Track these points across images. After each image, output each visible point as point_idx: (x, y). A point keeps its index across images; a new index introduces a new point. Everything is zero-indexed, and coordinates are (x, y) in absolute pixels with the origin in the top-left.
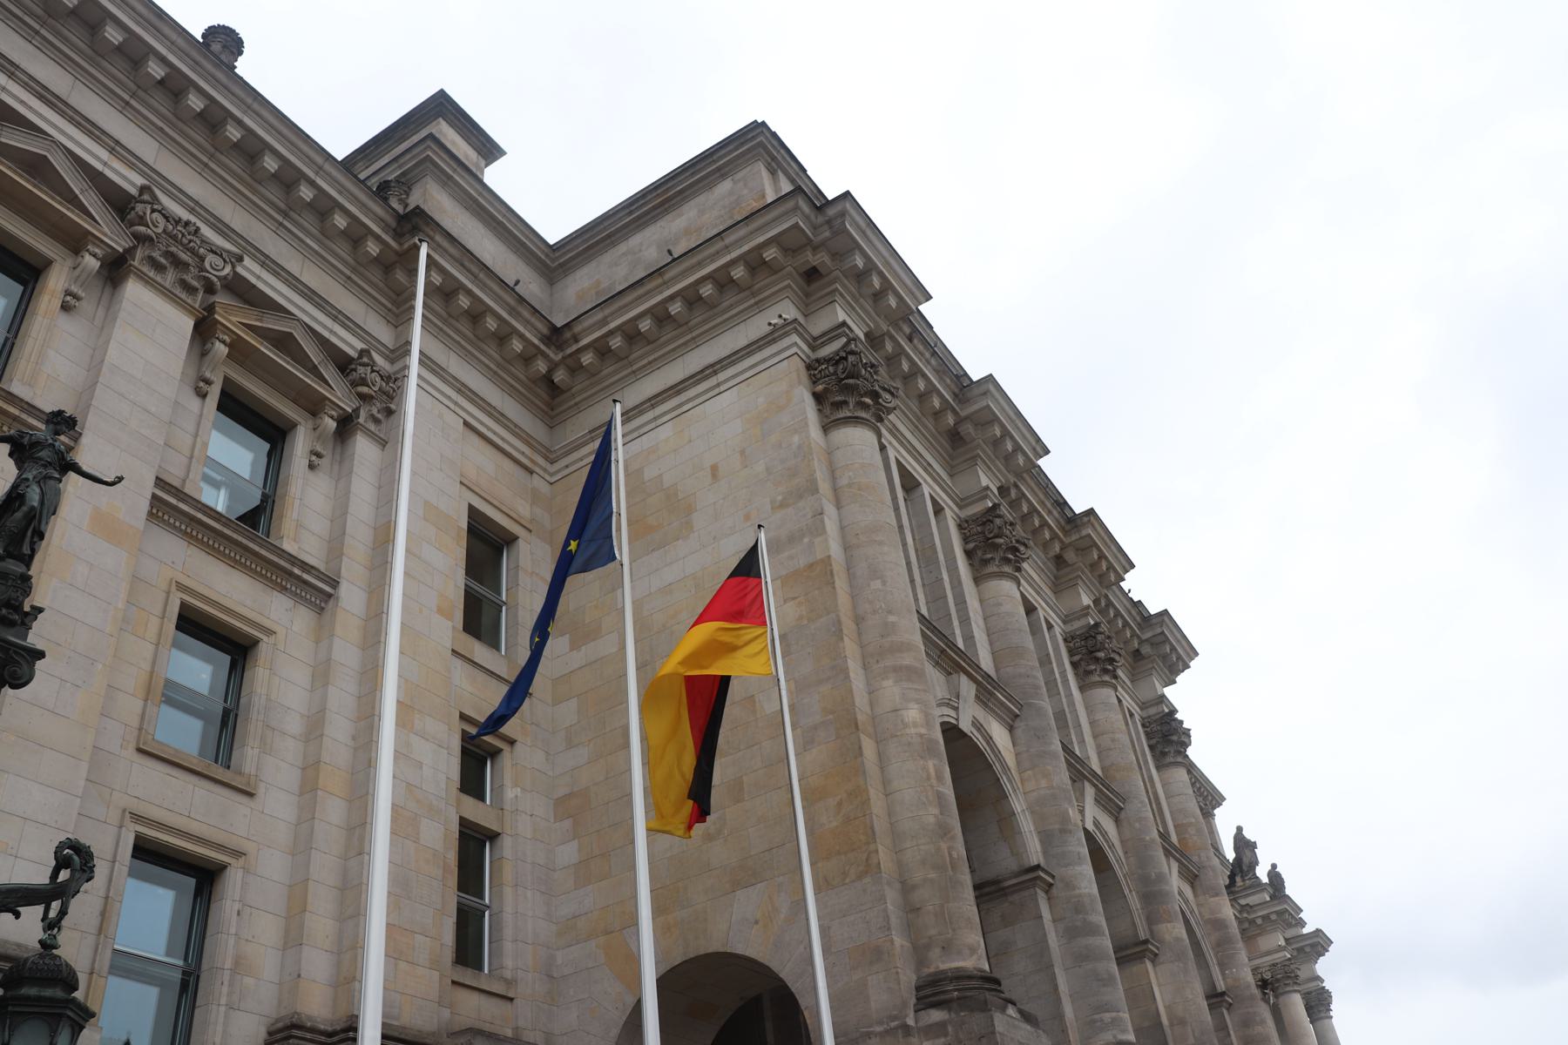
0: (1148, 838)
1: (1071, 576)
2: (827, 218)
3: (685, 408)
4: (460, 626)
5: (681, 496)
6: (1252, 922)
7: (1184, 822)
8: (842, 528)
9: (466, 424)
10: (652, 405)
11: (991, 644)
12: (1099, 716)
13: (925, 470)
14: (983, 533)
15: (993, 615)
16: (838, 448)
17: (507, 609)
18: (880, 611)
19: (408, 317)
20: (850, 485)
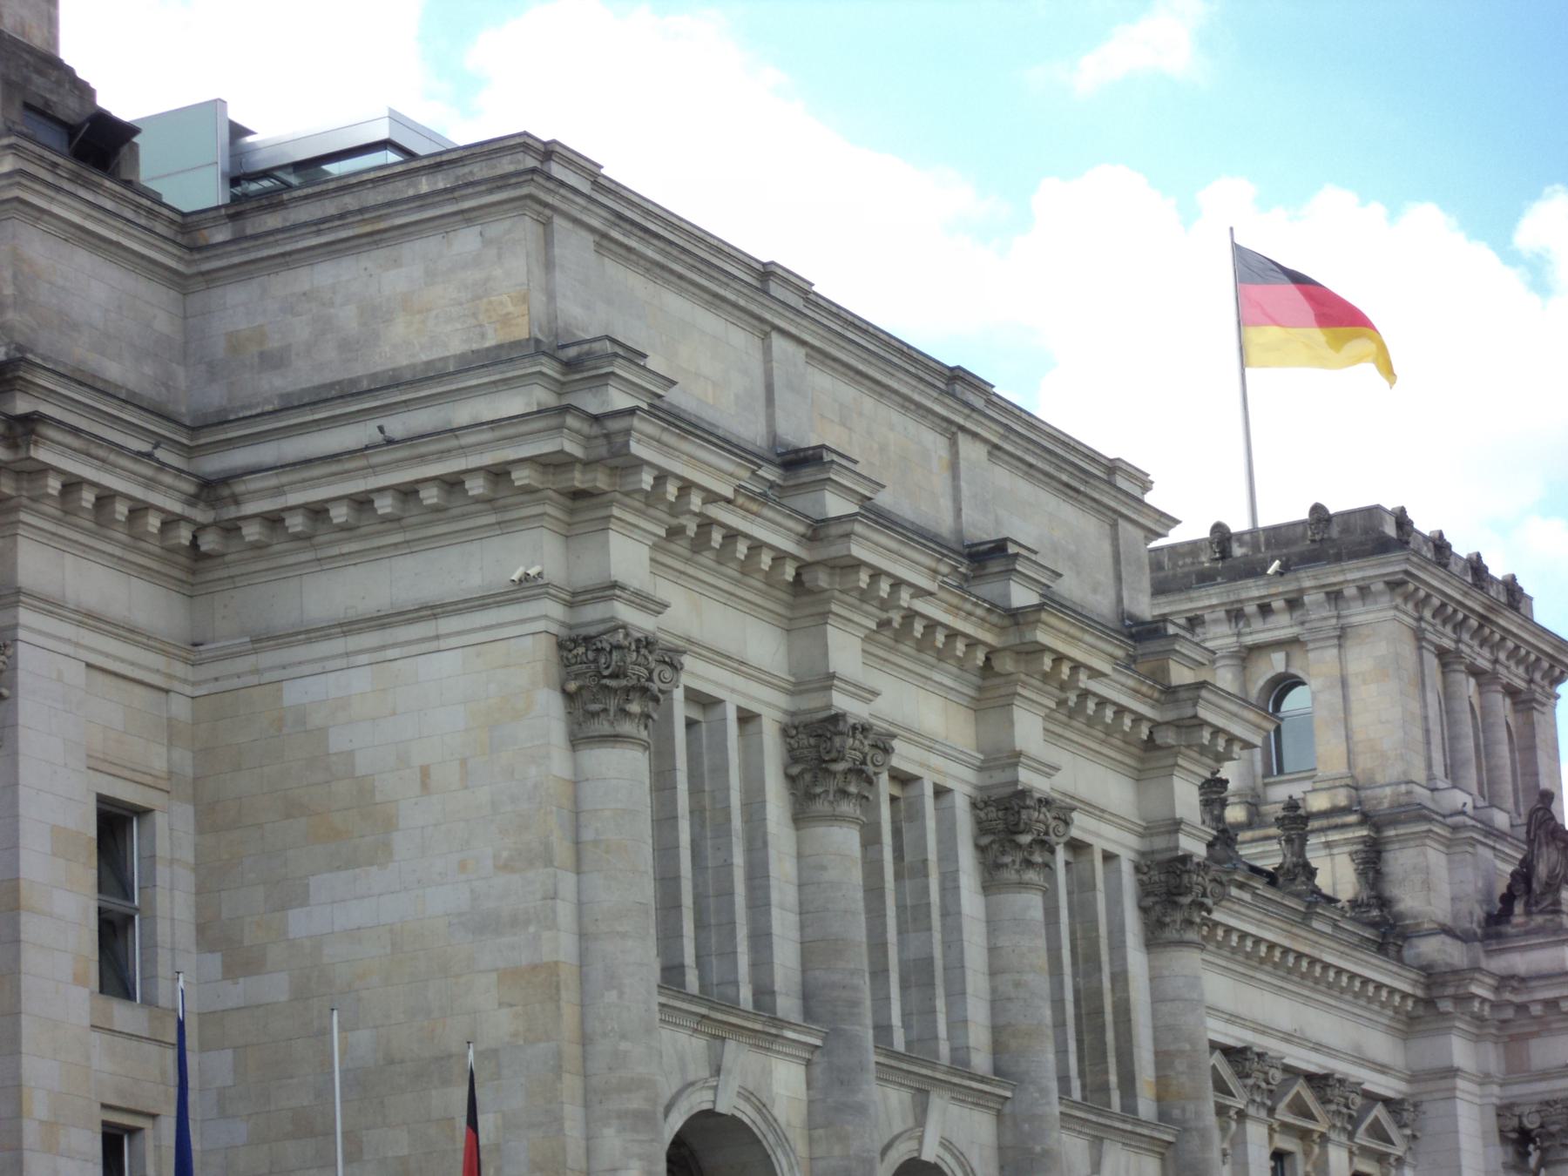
0: (1038, 1149)
1: (1003, 691)
2: (605, 431)
3: (391, 654)
4: (97, 989)
5: (378, 798)
6: (1522, 1008)
7: (1173, 1047)
8: (580, 904)
9: (89, 665)
10: (343, 632)
11: (802, 927)
12: (1004, 941)
13: (737, 671)
14: (817, 746)
15: (813, 884)
16: (587, 780)
17: (140, 920)
18: (611, 1035)
19: (14, 532)
20: (596, 843)
